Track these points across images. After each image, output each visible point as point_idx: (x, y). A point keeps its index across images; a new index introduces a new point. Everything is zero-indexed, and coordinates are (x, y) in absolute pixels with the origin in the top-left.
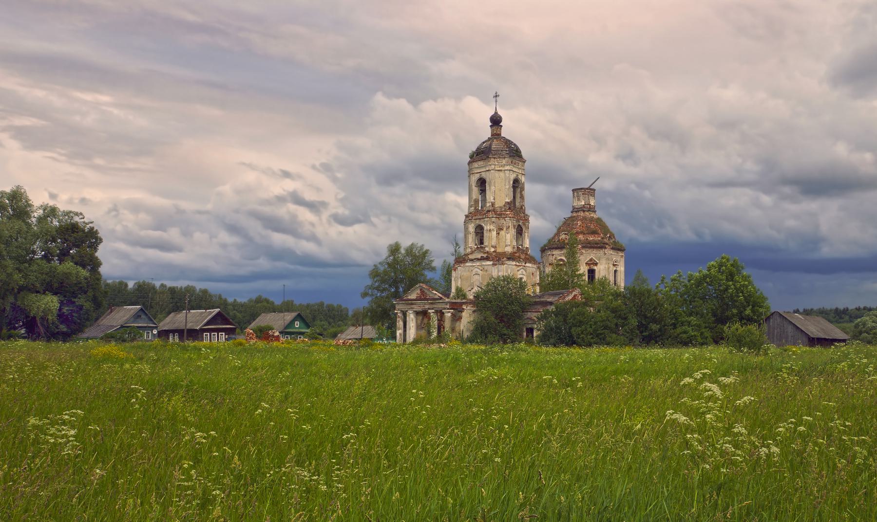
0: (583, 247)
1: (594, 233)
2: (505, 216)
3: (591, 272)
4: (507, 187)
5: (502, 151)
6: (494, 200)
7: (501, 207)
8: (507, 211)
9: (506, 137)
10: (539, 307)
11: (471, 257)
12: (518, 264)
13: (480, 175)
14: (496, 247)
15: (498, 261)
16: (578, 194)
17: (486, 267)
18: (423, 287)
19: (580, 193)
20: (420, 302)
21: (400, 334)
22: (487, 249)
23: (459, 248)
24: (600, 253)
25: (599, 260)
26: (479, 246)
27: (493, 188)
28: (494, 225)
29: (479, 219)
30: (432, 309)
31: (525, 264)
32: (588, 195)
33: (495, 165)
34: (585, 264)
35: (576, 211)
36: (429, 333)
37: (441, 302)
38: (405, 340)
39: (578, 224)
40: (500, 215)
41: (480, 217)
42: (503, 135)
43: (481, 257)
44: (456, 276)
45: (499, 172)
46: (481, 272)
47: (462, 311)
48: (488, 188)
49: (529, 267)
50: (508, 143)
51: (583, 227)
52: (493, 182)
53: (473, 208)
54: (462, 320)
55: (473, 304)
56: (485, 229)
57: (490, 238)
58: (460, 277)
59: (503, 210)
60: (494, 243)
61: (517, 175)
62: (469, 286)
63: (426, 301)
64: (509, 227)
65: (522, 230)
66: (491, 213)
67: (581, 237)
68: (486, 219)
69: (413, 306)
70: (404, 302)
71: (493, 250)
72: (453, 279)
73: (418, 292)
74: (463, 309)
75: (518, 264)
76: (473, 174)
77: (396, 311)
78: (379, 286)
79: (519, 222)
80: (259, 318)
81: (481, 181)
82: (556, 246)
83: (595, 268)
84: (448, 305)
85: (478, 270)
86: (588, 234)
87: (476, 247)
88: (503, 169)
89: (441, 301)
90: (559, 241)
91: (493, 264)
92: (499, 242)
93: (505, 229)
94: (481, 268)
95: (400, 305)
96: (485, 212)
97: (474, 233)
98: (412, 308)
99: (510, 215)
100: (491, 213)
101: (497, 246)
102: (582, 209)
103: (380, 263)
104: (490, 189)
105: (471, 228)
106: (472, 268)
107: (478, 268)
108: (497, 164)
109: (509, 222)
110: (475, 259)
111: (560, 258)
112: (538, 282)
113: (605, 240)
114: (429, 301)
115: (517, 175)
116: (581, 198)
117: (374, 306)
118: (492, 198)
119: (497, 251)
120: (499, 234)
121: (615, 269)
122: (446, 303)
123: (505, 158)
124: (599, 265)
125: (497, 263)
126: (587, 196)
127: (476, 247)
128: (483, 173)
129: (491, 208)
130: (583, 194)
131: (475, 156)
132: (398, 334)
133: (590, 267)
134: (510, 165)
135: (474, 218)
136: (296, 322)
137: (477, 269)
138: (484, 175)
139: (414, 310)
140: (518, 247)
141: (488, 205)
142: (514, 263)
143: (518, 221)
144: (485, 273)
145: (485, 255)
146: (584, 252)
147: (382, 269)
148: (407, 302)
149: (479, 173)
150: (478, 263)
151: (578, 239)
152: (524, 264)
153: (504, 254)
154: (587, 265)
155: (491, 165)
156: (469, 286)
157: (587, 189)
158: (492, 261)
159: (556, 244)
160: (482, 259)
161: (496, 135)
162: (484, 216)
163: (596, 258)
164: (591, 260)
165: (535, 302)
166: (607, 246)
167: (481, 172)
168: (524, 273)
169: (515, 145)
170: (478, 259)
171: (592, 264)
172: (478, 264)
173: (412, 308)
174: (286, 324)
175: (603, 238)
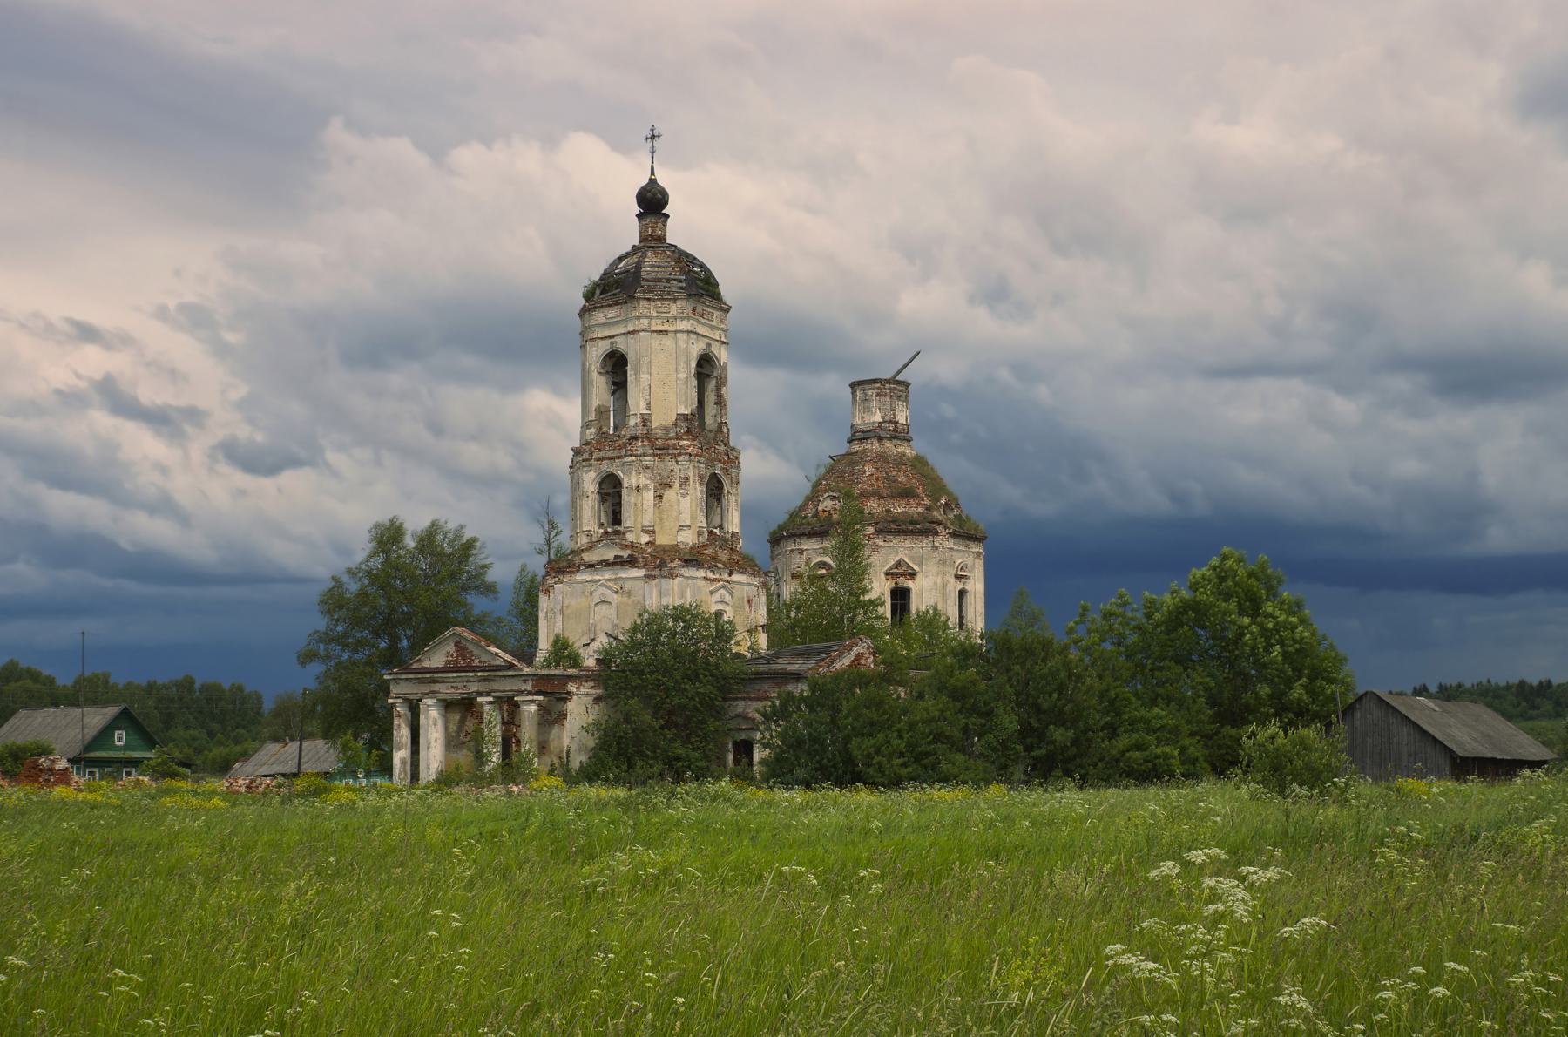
0: (879, 532)
1: (907, 494)
2: (676, 452)
3: (900, 597)
4: (683, 375)
5: (668, 281)
6: (650, 410)
7: (666, 429)
9: (680, 246)
10: (766, 687)
11: (588, 557)
12: (710, 575)
13: (612, 343)
14: (653, 532)
16: (866, 395)
17: (628, 585)
18: (465, 639)
19: (870, 392)
20: (455, 675)
21: (403, 762)
22: (630, 537)
23: (557, 534)
24: (922, 546)
25: (920, 564)
26: (609, 530)
27: (644, 377)
29: (610, 458)
30: (488, 694)
31: (730, 575)
32: (891, 397)
33: (650, 318)
34: (883, 576)
35: (861, 439)
36: (480, 757)
37: (513, 676)
38: (415, 776)
39: (865, 472)
40: (663, 449)
41: (611, 454)
43: (616, 557)
44: (552, 606)
45: (660, 337)
46: (615, 596)
47: (566, 697)
49: (740, 583)
50: (685, 260)
51: (877, 479)
52: (645, 362)
53: (593, 430)
54: (567, 723)
55: (593, 680)
56: (625, 485)
57: (639, 509)
58: (562, 611)
59: (672, 435)
60: (648, 519)
61: (709, 345)
62: (584, 634)
63: (471, 674)
64: (688, 479)
65: (722, 488)
66: (640, 443)
67: (873, 505)
68: (626, 459)
69: (436, 687)
71: (645, 539)
72: (541, 615)
74: (569, 693)
75: (710, 575)
76: (592, 340)
77: (390, 701)
78: (345, 635)
79: (713, 465)
80: (11, 721)
81: (614, 360)
82: (809, 528)
83: (910, 584)
84: (530, 683)
85: (608, 592)
86: (892, 496)
87: (602, 531)
88: (671, 329)
89: (510, 673)
90: (816, 515)
91: (645, 576)
92: (661, 520)
93: (676, 485)
94: (615, 587)
95: (402, 684)
97: (596, 496)
98: (433, 692)
99: (690, 450)
100: (640, 443)
101: (656, 529)
102: (875, 433)
103: (349, 571)
105: (590, 482)
106: (590, 587)
107: (608, 588)
108: (655, 314)
109: (689, 469)
110: (600, 563)
111: (820, 559)
112: (764, 621)
113: (935, 513)
114: (480, 674)
115: (709, 345)
116: (873, 404)
117: (333, 686)
118: (643, 405)
119: (657, 543)
120: (661, 497)
121: (960, 586)
122: (525, 678)
123: (675, 299)
124: (919, 577)
125: (656, 572)
126: (888, 399)
128: (616, 339)
129: (640, 431)
130: (878, 395)
131: (598, 292)
132: (397, 761)
133: (896, 583)
134: (689, 318)
135: (595, 455)
136: (116, 733)
137: (602, 590)
138: (621, 344)
139: (441, 696)
140: (711, 533)
141: (632, 422)
142: (701, 573)
143: (710, 464)
145: (625, 554)
146: (882, 544)
147: (353, 587)
148: (420, 676)
149: (610, 337)
150: (608, 574)
151: (866, 511)
152: (726, 576)
153: (674, 550)
154: (889, 577)
155: (638, 318)
156: (584, 634)
157: (888, 381)
158: (643, 567)
159: (809, 524)
160: (618, 562)
161: (653, 241)
162: (623, 452)
163: (910, 559)
164: (899, 564)
165: (757, 673)
166: (940, 529)
167: (614, 336)
168: (728, 598)
169: (702, 266)
170: (607, 564)
171: (902, 574)
172: (607, 577)
173: (433, 692)
174: (88, 738)
175: (928, 508)
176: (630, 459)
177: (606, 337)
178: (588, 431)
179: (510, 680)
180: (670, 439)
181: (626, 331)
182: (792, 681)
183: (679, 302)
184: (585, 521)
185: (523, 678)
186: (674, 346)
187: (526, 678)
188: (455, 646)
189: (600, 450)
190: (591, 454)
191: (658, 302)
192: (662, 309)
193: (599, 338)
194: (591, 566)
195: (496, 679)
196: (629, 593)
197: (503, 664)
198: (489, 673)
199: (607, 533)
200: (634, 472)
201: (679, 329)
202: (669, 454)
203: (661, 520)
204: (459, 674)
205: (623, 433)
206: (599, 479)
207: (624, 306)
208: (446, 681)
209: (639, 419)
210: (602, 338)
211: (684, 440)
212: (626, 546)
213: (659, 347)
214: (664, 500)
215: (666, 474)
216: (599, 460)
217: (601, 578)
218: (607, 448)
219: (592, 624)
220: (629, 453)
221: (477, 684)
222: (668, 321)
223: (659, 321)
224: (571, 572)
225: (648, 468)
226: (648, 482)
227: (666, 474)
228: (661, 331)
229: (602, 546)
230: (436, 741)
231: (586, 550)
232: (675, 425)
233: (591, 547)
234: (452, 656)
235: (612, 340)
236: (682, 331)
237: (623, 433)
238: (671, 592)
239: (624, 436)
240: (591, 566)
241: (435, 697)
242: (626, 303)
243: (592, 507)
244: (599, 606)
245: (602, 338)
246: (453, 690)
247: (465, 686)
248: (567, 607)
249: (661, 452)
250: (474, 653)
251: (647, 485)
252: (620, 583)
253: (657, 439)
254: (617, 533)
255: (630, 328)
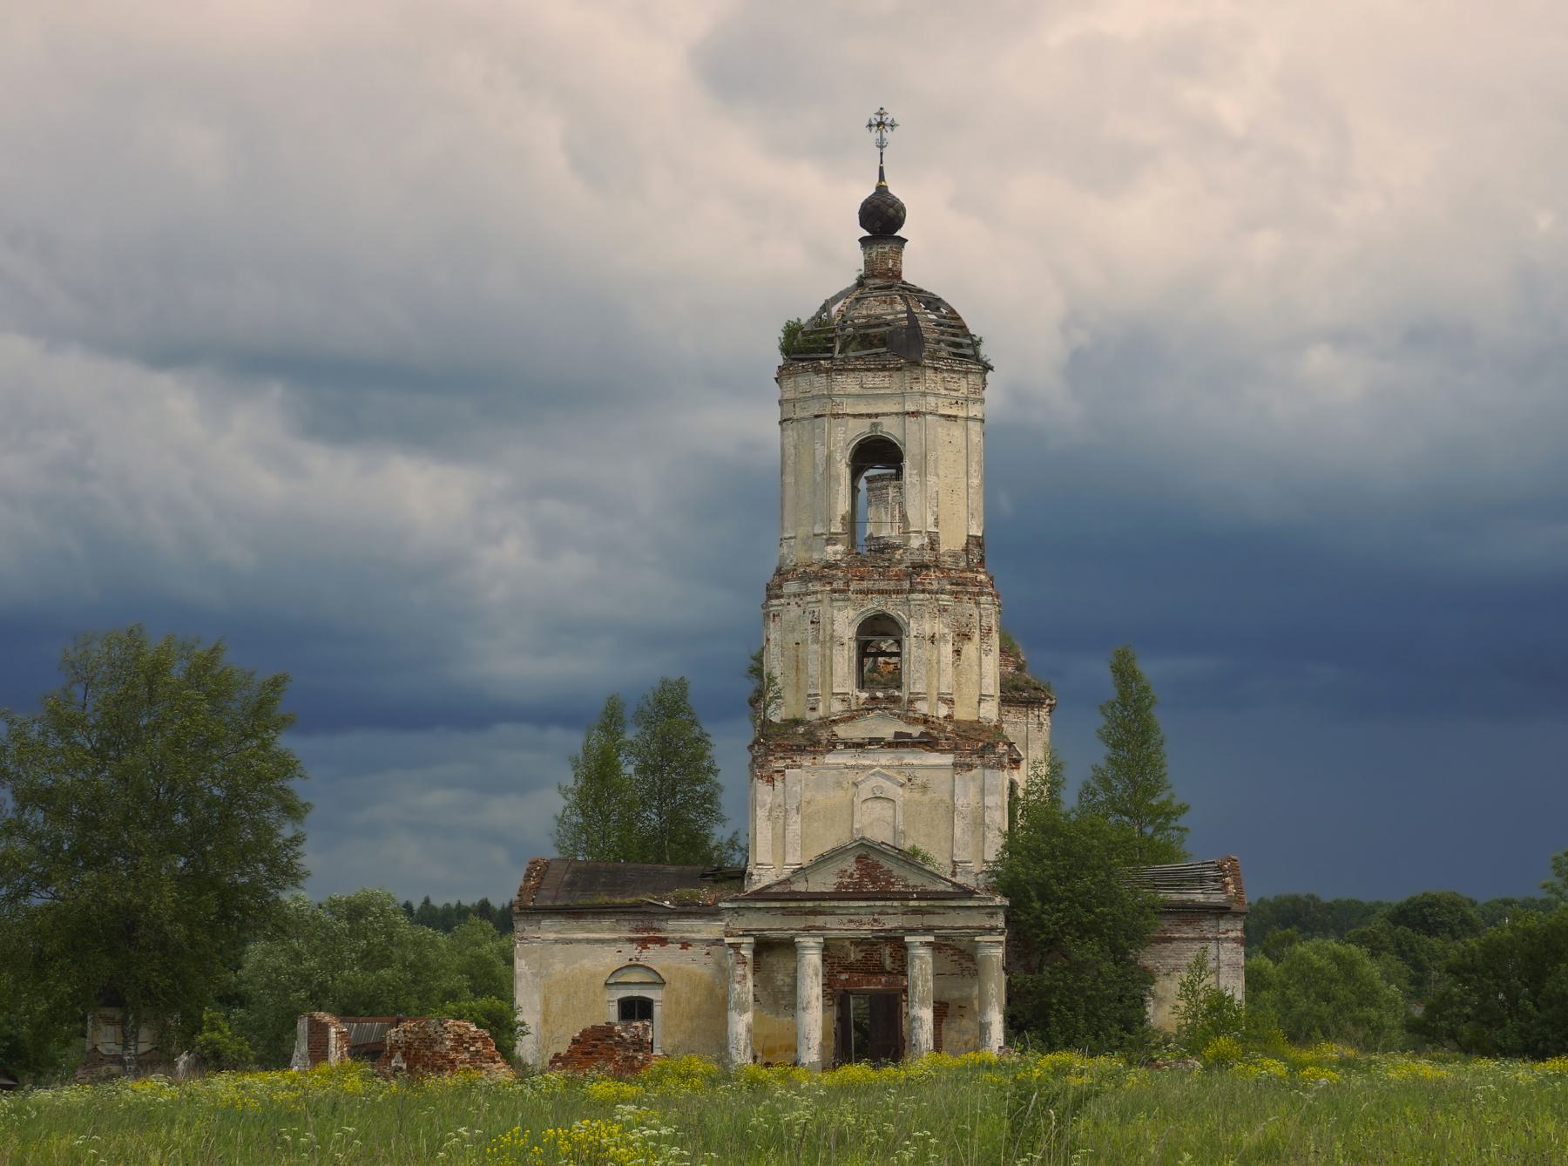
2: (976, 590)
6: (937, 526)
7: (954, 555)
8: (977, 572)
11: (842, 731)
13: (874, 425)
14: (952, 701)
15: (981, 753)
17: (921, 777)
22: (922, 708)
26: (880, 694)
27: (931, 479)
28: (947, 619)
29: (881, 592)
30: (928, 930)
40: (961, 587)
41: (883, 585)
42: (905, 277)
43: (897, 735)
44: (780, 800)
46: (900, 790)
48: (915, 479)
52: (931, 458)
53: (840, 547)
56: (913, 633)
57: (933, 667)
60: (946, 683)
63: (896, 904)
68: (914, 596)
69: (819, 921)
70: (778, 904)
71: (943, 711)
73: (844, 866)
76: (836, 416)
85: (887, 784)
87: (864, 695)
88: (962, 414)
89: (970, 903)
91: (955, 765)
92: (959, 685)
93: (976, 637)
94: (903, 779)
95: (749, 915)
96: (902, 567)
97: (854, 644)
104: (923, 484)
105: (845, 621)
106: (851, 776)
107: (887, 777)
108: (943, 392)
110: (872, 741)
125: (976, 760)
127: (864, 695)
128: (879, 419)
129: (928, 557)
135: (853, 586)
137: (875, 781)
138: (890, 428)
144: (917, 795)
145: (916, 731)
149: (869, 416)
150: (885, 758)
155: (924, 394)
158: (950, 751)
160: (900, 742)
162: (906, 585)
167: (877, 415)
173: (819, 929)
176: (921, 596)
177: (861, 415)
178: (829, 547)
179: (962, 913)
180: (962, 571)
181: (901, 410)
182: (1209, 917)
183: (971, 377)
184: (837, 679)
185: (988, 910)
186: (964, 438)
187: (994, 910)
188: (857, 862)
189: (862, 579)
190: (847, 584)
191: (946, 375)
192: (951, 385)
193: (848, 415)
194: (859, 746)
195: (937, 910)
196: (925, 788)
197: (951, 890)
198: (930, 903)
199: (874, 699)
200: (927, 616)
201: (971, 415)
202: (967, 592)
203: (959, 685)
204: (871, 903)
205: (898, 557)
206: (860, 620)
207: (895, 374)
208: (838, 912)
209: (926, 540)
210: (854, 416)
211: (980, 573)
212: (916, 720)
213: (947, 439)
214: (962, 657)
215: (964, 620)
216: (861, 592)
217: (875, 763)
218: (876, 577)
219: (857, 829)
220: (920, 587)
221: (901, 917)
222: (957, 403)
223: (947, 402)
224: (814, 752)
225: (945, 610)
226: (946, 631)
227: (964, 620)
228: (949, 416)
229: (872, 718)
230: (818, 998)
231: (843, 720)
232: (966, 550)
233: (851, 718)
234: (851, 876)
235: (874, 420)
236: (974, 419)
237: (898, 557)
238: (1000, 787)
239: (900, 562)
240: (859, 746)
241: (822, 935)
242: (899, 369)
243: (850, 659)
244: (869, 804)
245: (854, 416)
246: (852, 926)
247: (875, 920)
248: (809, 803)
249: (959, 588)
250: (894, 873)
251: (944, 635)
252: (908, 772)
253: (950, 570)
254: (895, 700)
255: (910, 407)
